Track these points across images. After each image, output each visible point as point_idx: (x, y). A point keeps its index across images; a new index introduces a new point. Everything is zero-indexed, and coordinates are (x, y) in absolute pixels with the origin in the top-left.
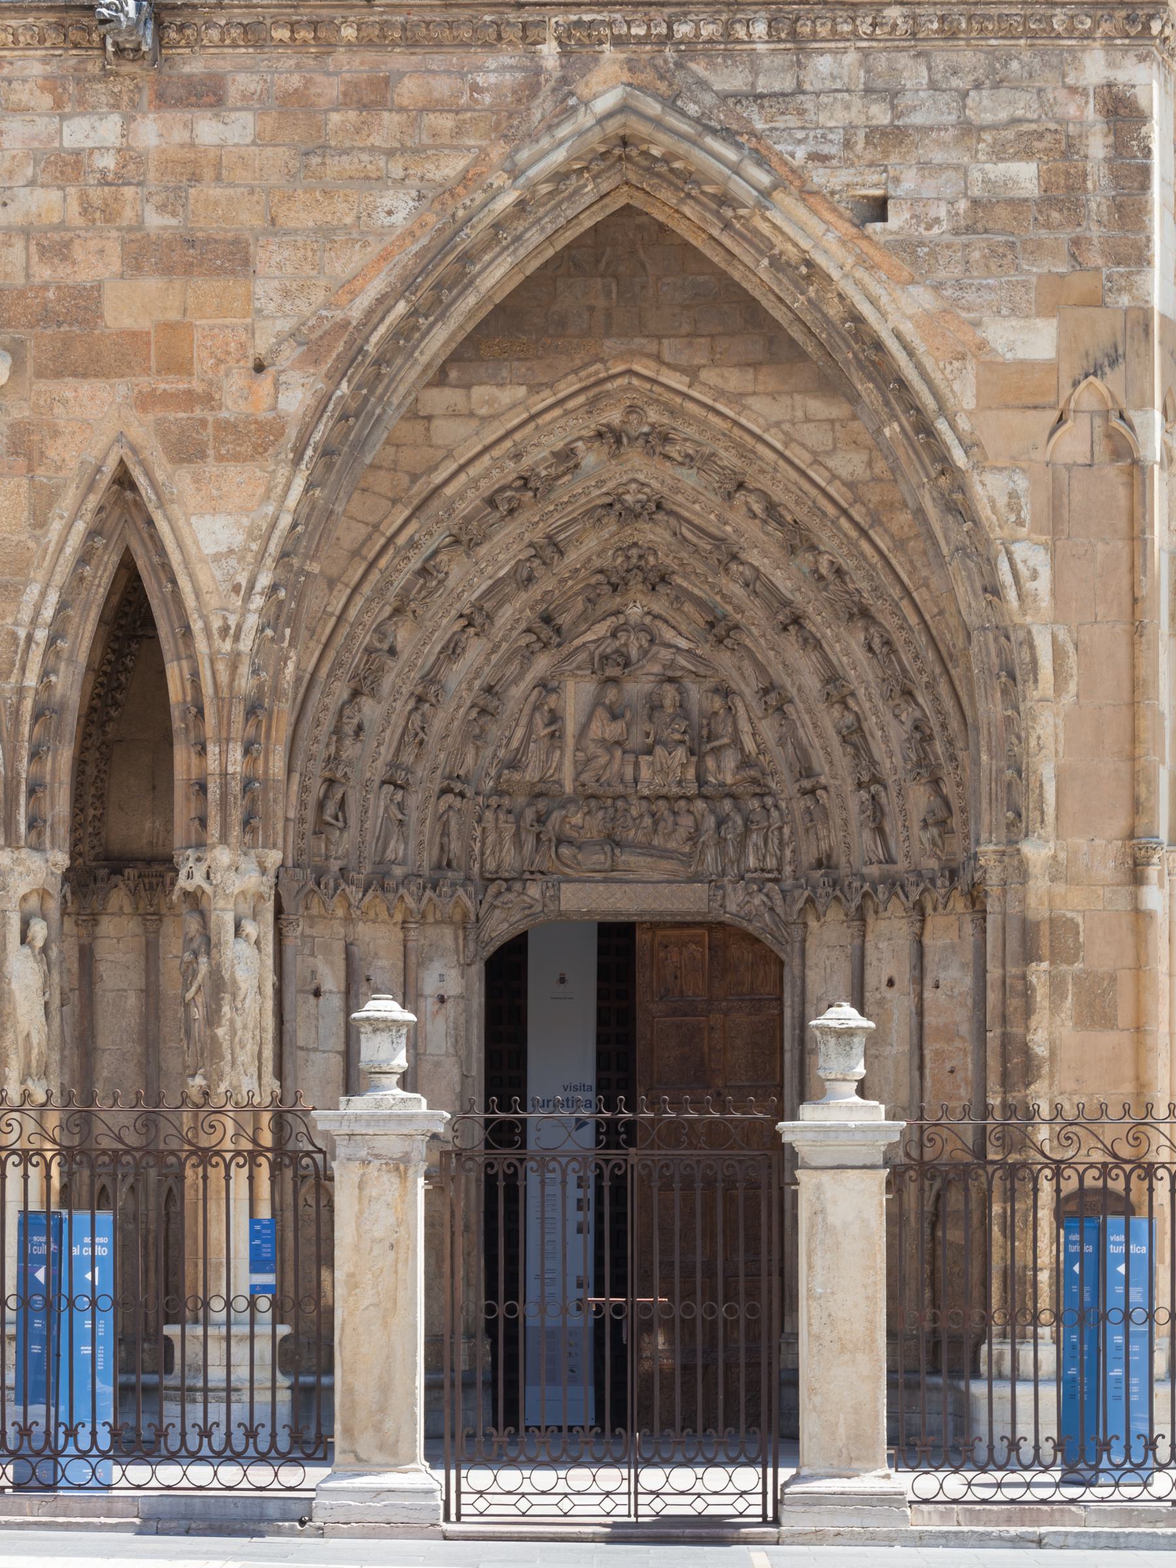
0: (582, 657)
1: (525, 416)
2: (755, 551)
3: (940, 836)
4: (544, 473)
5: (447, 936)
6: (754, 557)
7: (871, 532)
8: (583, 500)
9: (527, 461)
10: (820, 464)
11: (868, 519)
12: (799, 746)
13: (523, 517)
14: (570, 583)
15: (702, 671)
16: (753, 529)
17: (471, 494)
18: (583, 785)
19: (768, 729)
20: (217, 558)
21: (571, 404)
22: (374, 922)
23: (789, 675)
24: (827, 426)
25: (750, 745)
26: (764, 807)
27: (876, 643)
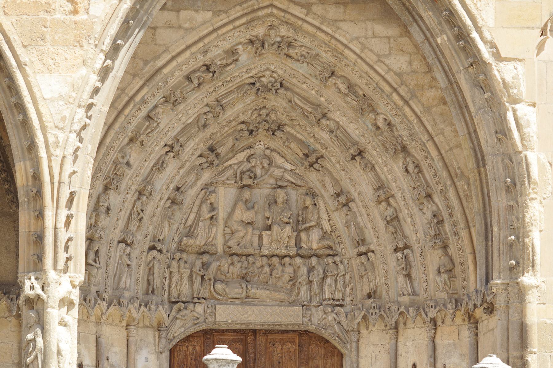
0: (230, 172)
1: (211, 29)
2: (338, 113)
3: (449, 279)
4: (219, 63)
5: (150, 336)
6: (337, 116)
7: (411, 102)
8: (239, 80)
9: (210, 55)
10: (382, 62)
11: (409, 94)
12: (357, 226)
13: (205, 88)
14: (226, 129)
15: (299, 183)
16: (338, 100)
17: (177, 73)
18: (230, 248)
19: (339, 218)
20: (52, 100)
21: (238, 23)
22: (111, 325)
23: (354, 186)
24: (386, 40)
25: (327, 227)
26: (334, 262)
27: (411, 167)
